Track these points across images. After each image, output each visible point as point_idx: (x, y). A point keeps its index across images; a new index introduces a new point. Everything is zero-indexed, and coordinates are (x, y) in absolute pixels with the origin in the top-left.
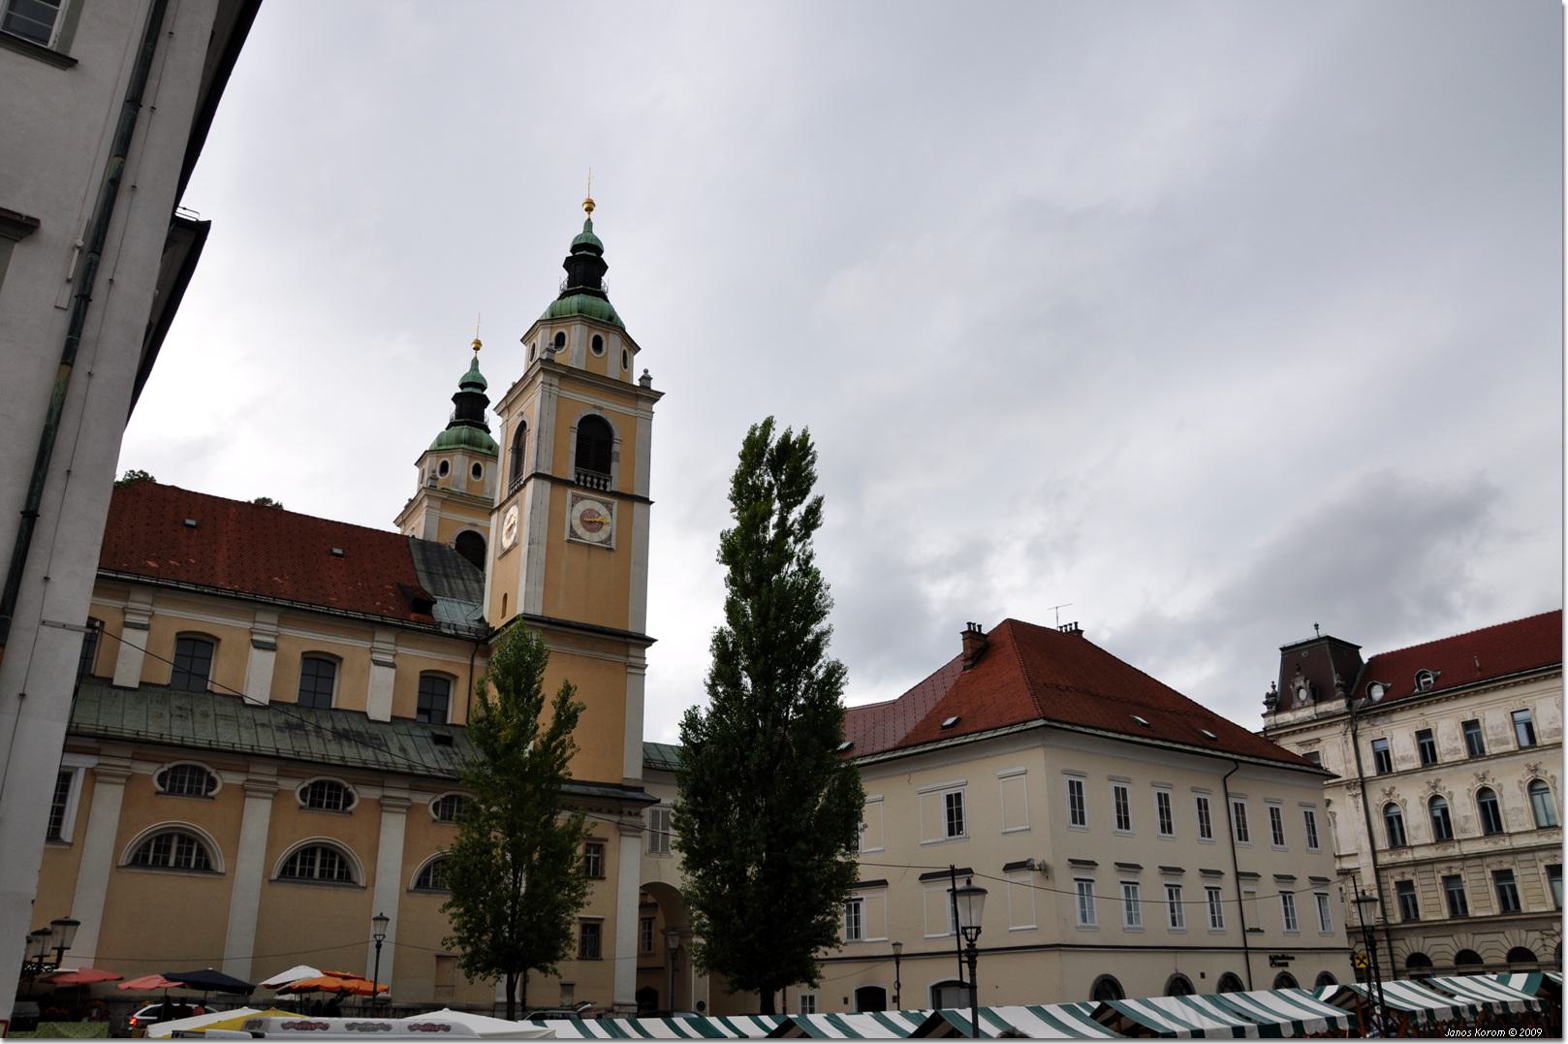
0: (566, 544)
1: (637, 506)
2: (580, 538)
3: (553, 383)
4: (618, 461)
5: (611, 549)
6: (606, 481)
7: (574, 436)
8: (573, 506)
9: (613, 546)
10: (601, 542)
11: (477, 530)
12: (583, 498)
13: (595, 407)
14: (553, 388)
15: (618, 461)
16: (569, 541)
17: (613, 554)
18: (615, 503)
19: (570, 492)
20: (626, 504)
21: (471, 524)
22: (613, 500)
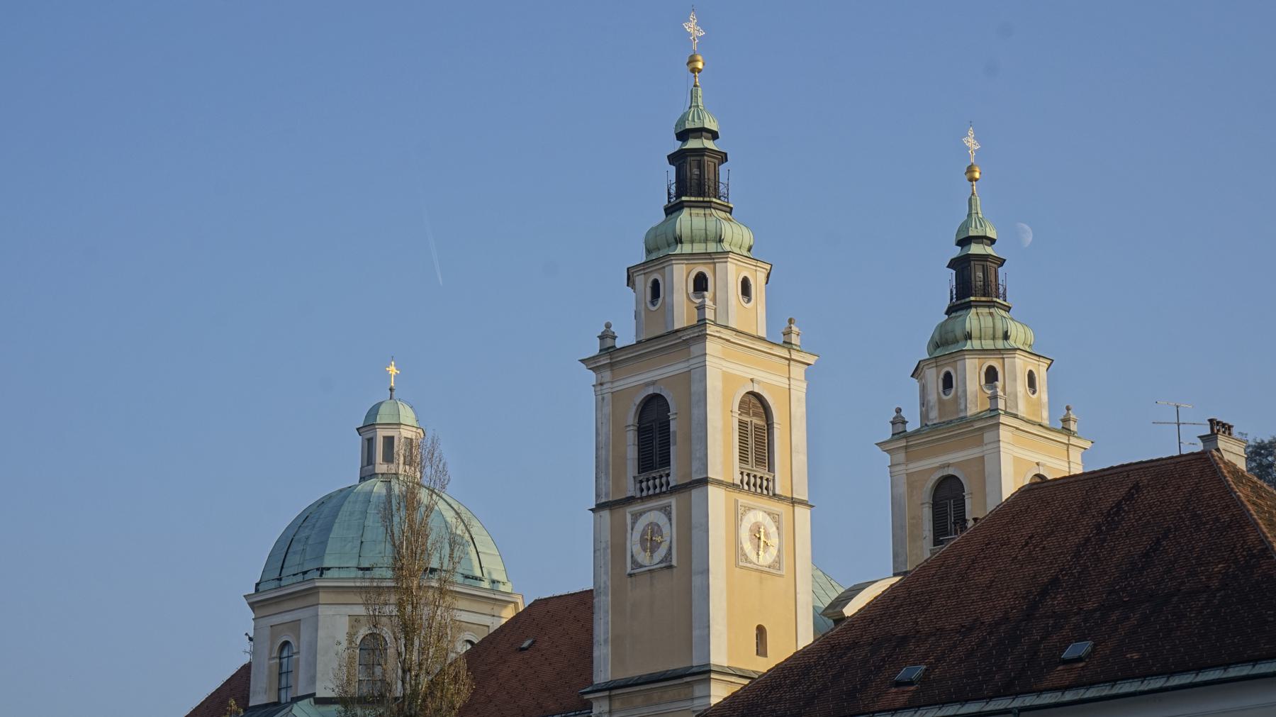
0: (629, 579)
1: (695, 493)
2: (641, 566)
3: (604, 380)
4: (675, 444)
5: (671, 567)
6: (668, 475)
7: (631, 437)
8: (632, 529)
9: (674, 563)
10: (661, 562)
11: (951, 471)
12: (641, 514)
13: (647, 385)
14: (605, 386)
15: (675, 444)
16: (630, 575)
17: (675, 570)
18: (673, 501)
19: (629, 511)
20: (684, 496)
21: (943, 467)
22: (670, 500)
